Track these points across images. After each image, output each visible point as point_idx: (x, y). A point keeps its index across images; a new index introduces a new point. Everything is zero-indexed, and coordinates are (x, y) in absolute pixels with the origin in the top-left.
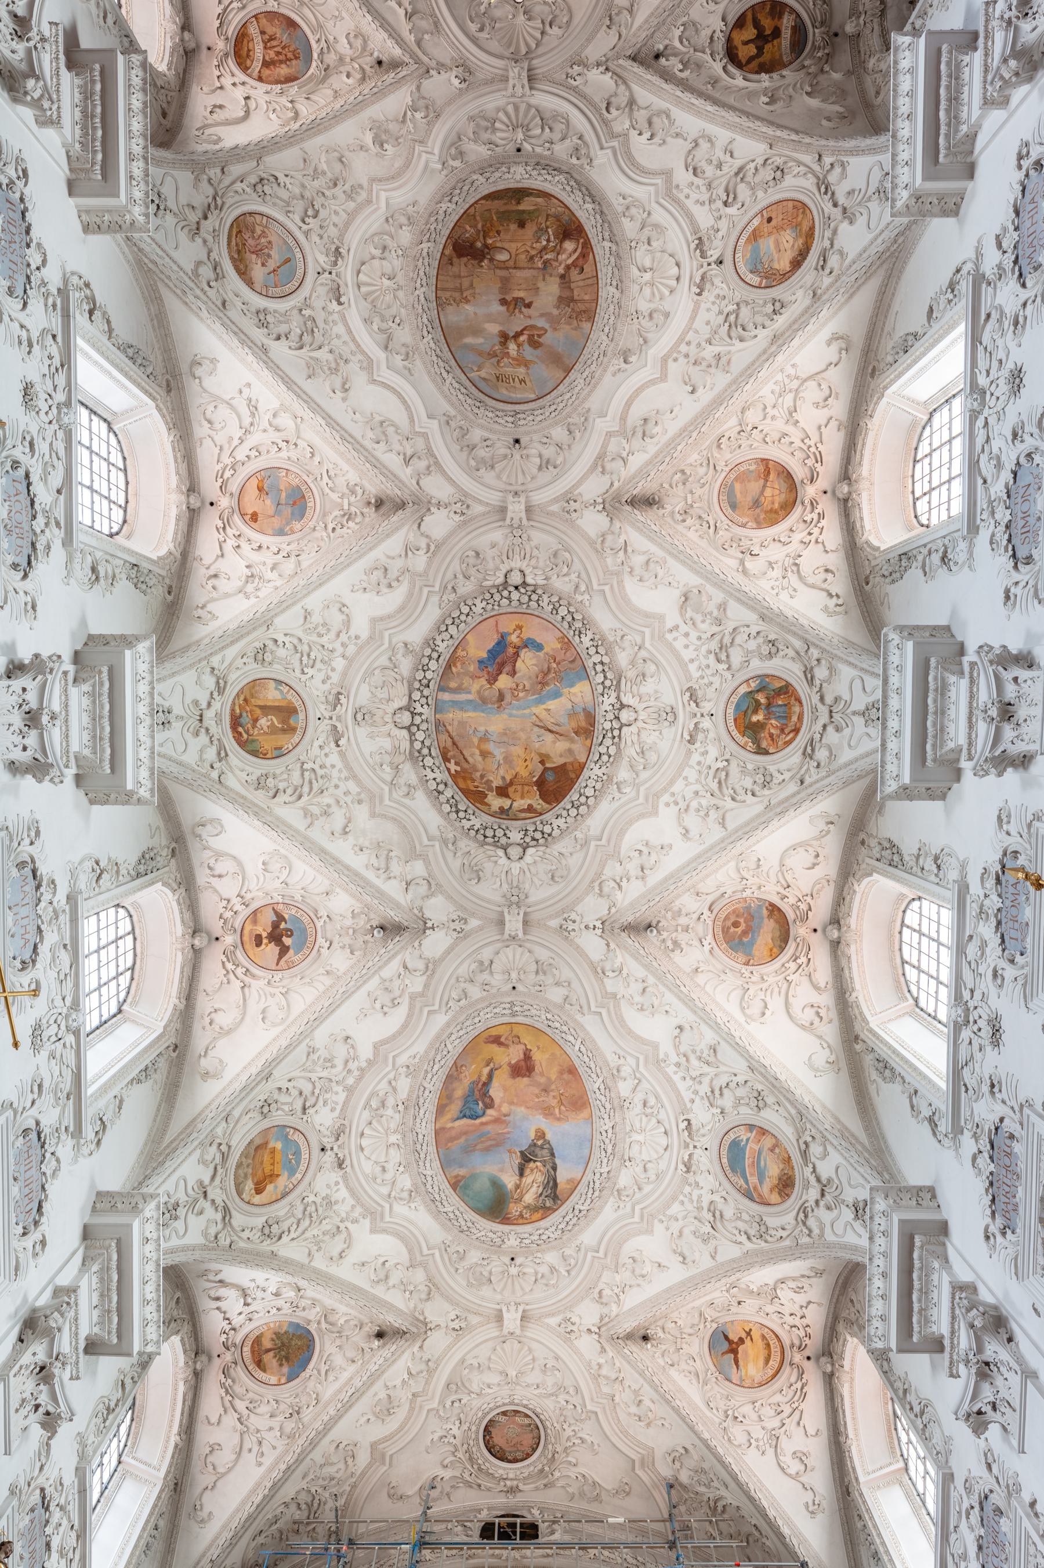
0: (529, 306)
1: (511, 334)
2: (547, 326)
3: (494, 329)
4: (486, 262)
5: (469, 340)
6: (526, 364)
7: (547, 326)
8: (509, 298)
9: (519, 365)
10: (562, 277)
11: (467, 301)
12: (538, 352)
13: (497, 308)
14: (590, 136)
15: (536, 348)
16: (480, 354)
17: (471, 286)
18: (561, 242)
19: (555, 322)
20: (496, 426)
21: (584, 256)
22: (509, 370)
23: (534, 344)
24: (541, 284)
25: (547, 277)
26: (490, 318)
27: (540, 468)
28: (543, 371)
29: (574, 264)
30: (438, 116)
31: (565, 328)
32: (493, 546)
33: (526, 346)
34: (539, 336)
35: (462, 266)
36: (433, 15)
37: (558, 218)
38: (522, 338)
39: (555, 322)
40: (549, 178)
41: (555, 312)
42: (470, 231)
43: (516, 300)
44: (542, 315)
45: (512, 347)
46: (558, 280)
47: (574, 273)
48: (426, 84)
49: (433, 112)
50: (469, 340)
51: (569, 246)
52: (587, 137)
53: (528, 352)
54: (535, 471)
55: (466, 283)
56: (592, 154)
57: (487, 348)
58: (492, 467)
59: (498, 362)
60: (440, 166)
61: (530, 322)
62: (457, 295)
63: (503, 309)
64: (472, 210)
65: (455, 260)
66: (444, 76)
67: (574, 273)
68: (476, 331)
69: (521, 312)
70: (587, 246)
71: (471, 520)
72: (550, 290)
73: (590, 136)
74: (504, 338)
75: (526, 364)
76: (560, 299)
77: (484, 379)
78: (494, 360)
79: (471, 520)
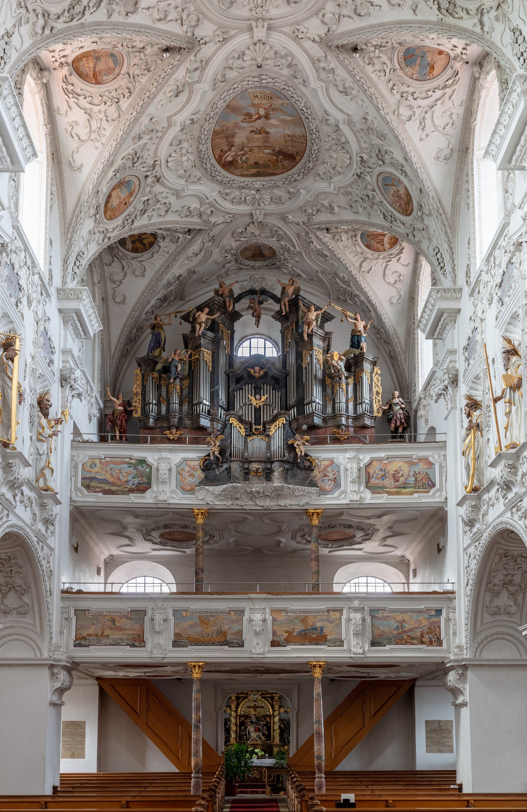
0: (252, 131)
1: (263, 119)
2: (241, 124)
3: (273, 121)
4: (278, 149)
5: (288, 118)
6: (253, 105)
7: (241, 124)
8: (264, 134)
9: (258, 104)
10: (232, 146)
11: (289, 136)
12: (246, 111)
13: (272, 131)
14: (220, 201)
15: (248, 113)
16: (282, 111)
17: (286, 141)
18: (234, 159)
19: (236, 126)
20: (273, 75)
21: (221, 157)
22: (264, 102)
23: (249, 115)
24: (245, 141)
25: (241, 144)
26: (275, 126)
27: (244, 54)
28: (244, 103)
29: (226, 152)
30: (300, 208)
31: (230, 124)
32: (277, 6)
33: (253, 113)
34: (246, 119)
35: (291, 150)
36: (300, 240)
37: (236, 168)
38: (256, 117)
39: (236, 126)
40: (242, 184)
41: (236, 131)
42: (286, 163)
43: (260, 133)
44: (244, 128)
45: (262, 112)
46: (235, 144)
47: (226, 148)
48: (305, 220)
49: (303, 210)
50: (288, 118)
51: (230, 159)
52: (222, 199)
53: (252, 111)
54: (247, 52)
55: (289, 143)
56: (219, 195)
57: (277, 113)
58: (276, 53)
59: (271, 106)
60: (301, 190)
61: (251, 124)
62: (294, 139)
63: (267, 130)
64: (284, 171)
65: (295, 153)
66: (296, 220)
67: (226, 148)
68: (284, 121)
69: (257, 129)
70: (219, 160)
71: (292, 24)
72: (240, 138)
73: (220, 201)
74: (267, 117)
75: (253, 105)
76: (233, 136)
77: (280, 99)
78: (273, 107)
79: (292, 24)
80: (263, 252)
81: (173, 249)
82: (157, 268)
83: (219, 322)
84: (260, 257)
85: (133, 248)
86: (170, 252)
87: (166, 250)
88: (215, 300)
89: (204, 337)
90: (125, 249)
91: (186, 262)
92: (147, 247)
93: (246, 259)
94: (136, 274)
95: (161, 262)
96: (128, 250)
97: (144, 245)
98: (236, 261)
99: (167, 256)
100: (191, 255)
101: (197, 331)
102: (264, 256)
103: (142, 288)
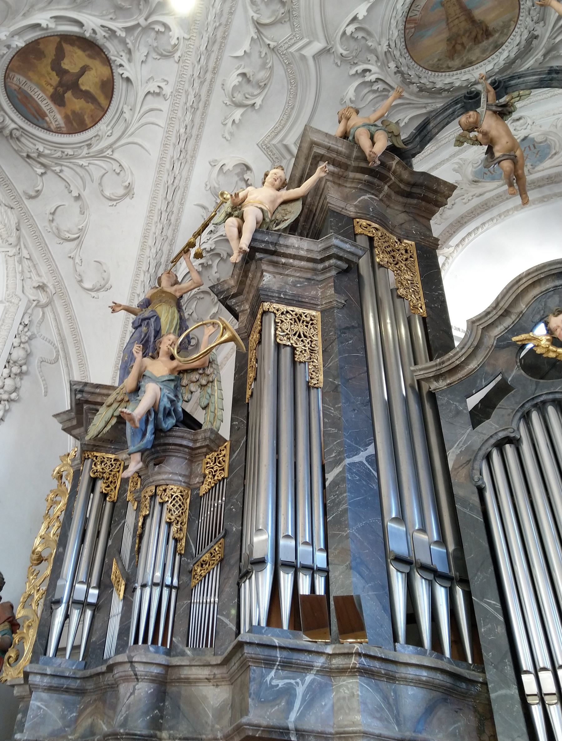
80: (477, 14)
81: (172, 79)
82: (155, 154)
83: (351, 211)
84: (476, 41)
85: (67, 118)
86: (167, 90)
87: (152, 87)
88: (313, 144)
89: (275, 264)
90: (49, 130)
91: (237, 114)
92: (102, 100)
93: (437, 69)
94: (107, 193)
95: (160, 133)
96: (58, 131)
97: (88, 96)
98: (406, 81)
99: (165, 106)
100: (234, 80)
101: (234, 243)
102: (487, 33)
103: (139, 231)
